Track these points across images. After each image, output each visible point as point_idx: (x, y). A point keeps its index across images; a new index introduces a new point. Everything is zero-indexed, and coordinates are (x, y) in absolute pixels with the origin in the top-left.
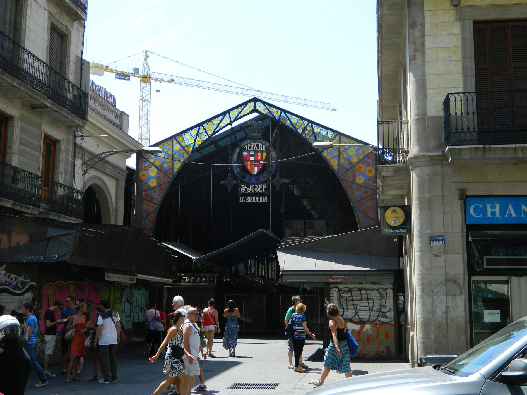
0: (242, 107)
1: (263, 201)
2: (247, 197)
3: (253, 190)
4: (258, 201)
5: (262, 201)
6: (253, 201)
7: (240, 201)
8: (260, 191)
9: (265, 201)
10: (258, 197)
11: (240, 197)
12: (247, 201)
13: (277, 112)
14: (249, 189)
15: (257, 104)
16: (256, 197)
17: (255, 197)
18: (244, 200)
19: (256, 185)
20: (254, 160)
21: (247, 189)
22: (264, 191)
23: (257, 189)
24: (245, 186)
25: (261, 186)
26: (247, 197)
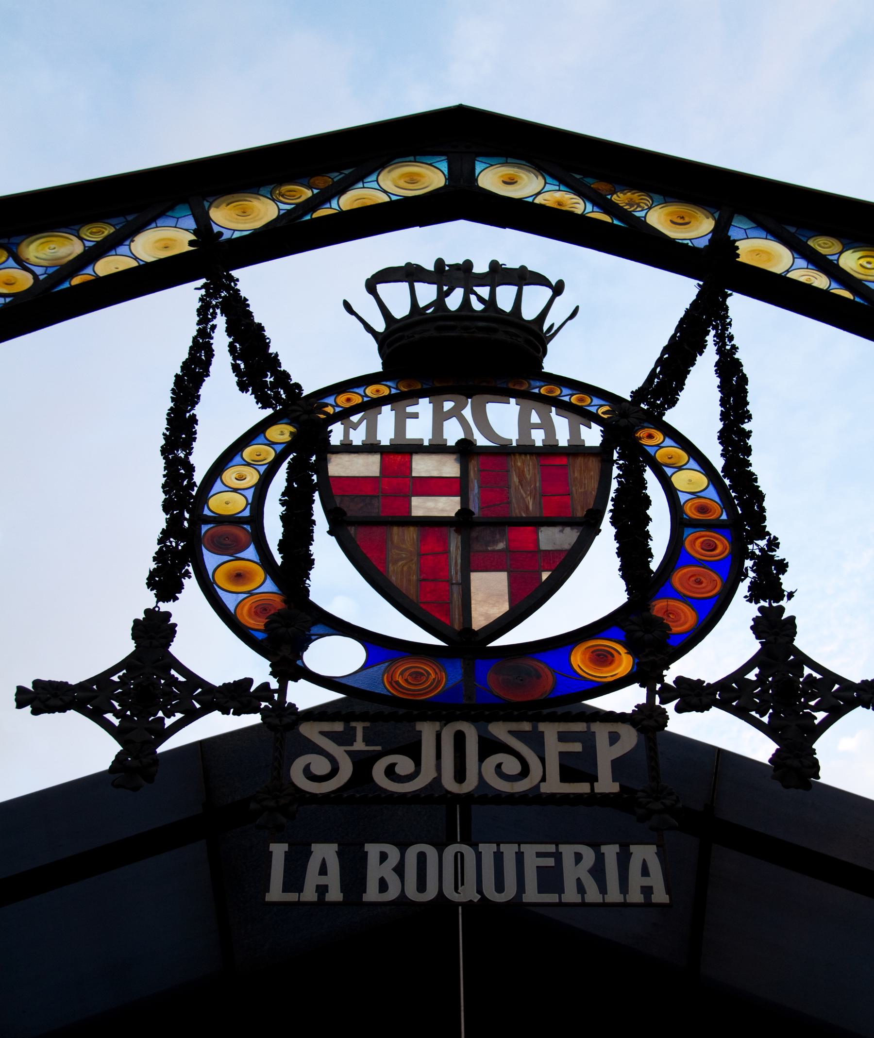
0: (336, 176)
1: (614, 895)
2: (373, 850)
3: (460, 775)
4: (532, 895)
5: (593, 895)
6: (468, 894)
7: (276, 893)
8: (554, 785)
9: (635, 896)
10: (530, 850)
11: (279, 851)
12: (372, 894)
13: (682, 222)
14: (404, 765)
15: (479, 167)
16: (509, 851)
17: (488, 850)
18: (333, 879)
19: (500, 731)
20: (464, 516)
21: (378, 772)
22: (606, 784)
23: (512, 766)
24: (344, 739)
25: (563, 737)
26: (373, 850)
